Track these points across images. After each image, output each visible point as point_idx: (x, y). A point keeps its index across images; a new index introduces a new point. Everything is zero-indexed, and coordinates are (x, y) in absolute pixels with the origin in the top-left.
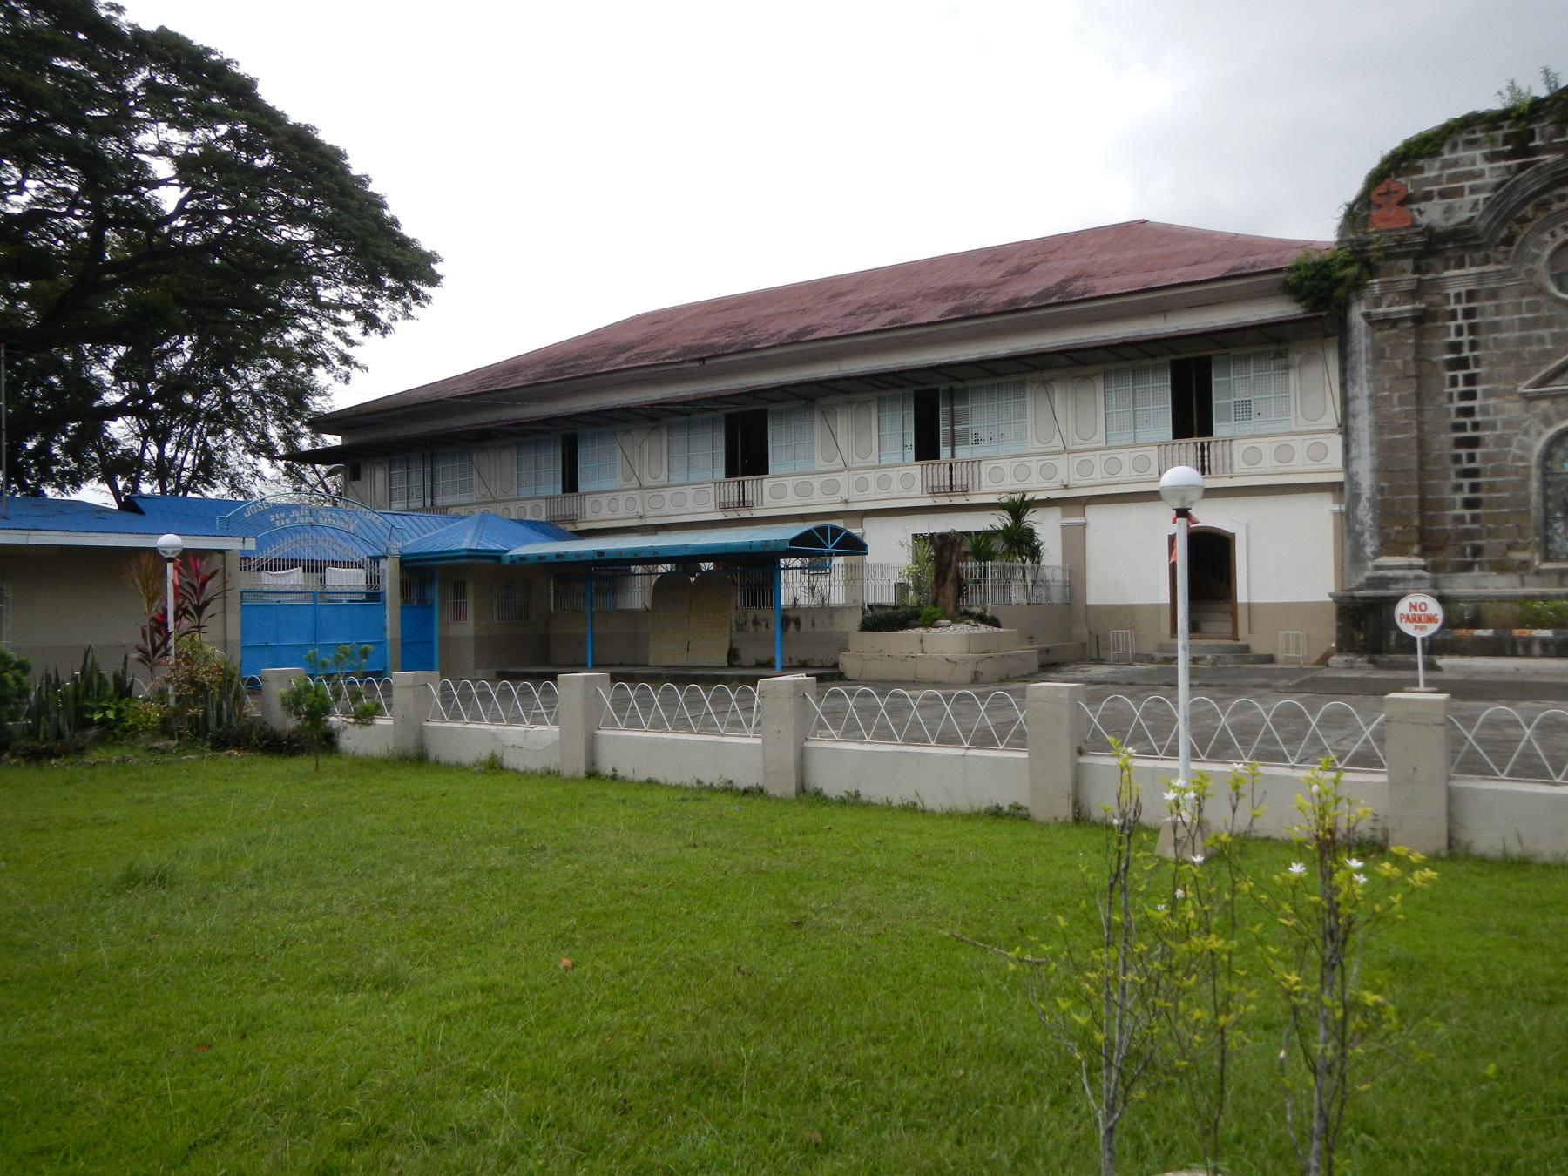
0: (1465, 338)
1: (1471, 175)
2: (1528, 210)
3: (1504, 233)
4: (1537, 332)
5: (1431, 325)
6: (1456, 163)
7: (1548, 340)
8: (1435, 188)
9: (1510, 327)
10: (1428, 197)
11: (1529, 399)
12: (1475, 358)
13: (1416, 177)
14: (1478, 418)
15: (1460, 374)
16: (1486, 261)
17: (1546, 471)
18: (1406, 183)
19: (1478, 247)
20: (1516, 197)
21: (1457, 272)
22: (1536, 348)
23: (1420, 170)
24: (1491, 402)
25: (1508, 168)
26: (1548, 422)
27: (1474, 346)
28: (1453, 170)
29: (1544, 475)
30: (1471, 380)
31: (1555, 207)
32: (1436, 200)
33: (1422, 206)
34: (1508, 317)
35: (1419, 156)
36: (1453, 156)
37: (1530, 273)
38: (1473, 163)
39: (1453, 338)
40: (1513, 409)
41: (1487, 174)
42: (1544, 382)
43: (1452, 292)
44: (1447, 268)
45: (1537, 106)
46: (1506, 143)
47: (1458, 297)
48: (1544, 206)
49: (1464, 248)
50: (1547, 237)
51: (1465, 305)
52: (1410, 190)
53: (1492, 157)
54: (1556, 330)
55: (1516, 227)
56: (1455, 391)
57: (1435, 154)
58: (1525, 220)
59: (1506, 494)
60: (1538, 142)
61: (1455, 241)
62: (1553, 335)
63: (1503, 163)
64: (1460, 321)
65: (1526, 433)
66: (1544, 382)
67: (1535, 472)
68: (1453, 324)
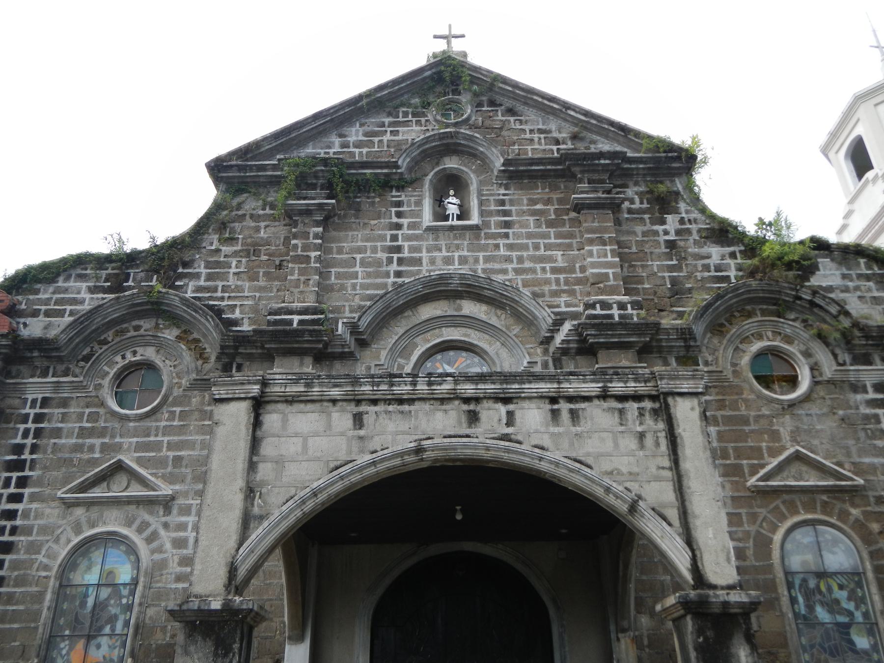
0: (29, 441)
1: (74, 301)
2: (110, 335)
3: (87, 351)
4: (89, 441)
5: (5, 426)
6: (66, 290)
7: (97, 449)
8: (43, 308)
9: (70, 435)
10: (35, 314)
11: (69, 505)
12: (32, 460)
13: (31, 297)
14: (18, 522)
15: (15, 475)
16: (66, 374)
17: (64, 585)
18: (23, 301)
19: (60, 359)
20: (98, 321)
21: (40, 380)
22: (86, 456)
23: (37, 292)
24: (34, 506)
25: (103, 299)
26: (78, 530)
27: (34, 449)
28: (62, 296)
29: (61, 586)
30: (22, 482)
31: (132, 333)
32: (41, 317)
33: (29, 320)
34: (68, 425)
35: (39, 281)
36: (66, 285)
37: (99, 387)
38: (79, 293)
39: (19, 440)
40: (51, 513)
41: (87, 302)
42: (84, 487)
43: (30, 397)
44: (32, 376)
45: (132, 259)
46: (106, 280)
47: (34, 401)
48: (123, 332)
49: (49, 358)
50: (118, 358)
51: (38, 410)
52: (23, 307)
53: (92, 290)
54: (106, 440)
55: (97, 347)
56: (6, 492)
57: (53, 280)
58: (105, 342)
59: (21, 607)
60: (131, 283)
61: (40, 350)
62: (103, 444)
63: (101, 296)
64: (30, 425)
65: (57, 540)
66: (84, 487)
67: (52, 583)
68: (22, 427)
